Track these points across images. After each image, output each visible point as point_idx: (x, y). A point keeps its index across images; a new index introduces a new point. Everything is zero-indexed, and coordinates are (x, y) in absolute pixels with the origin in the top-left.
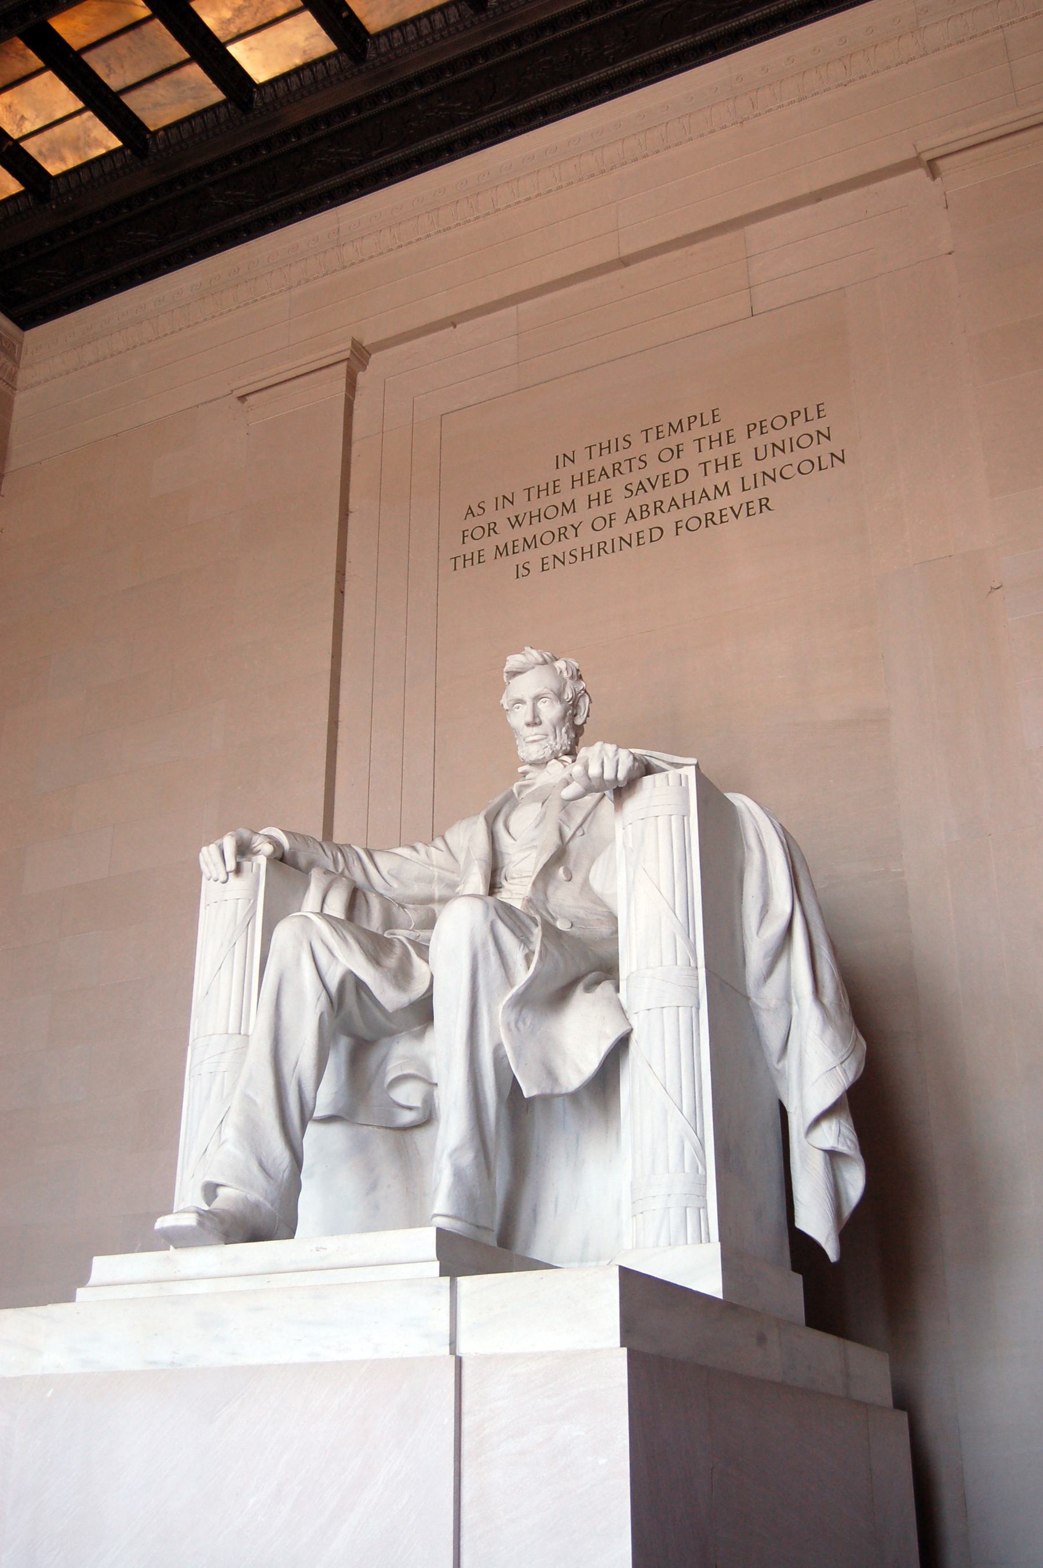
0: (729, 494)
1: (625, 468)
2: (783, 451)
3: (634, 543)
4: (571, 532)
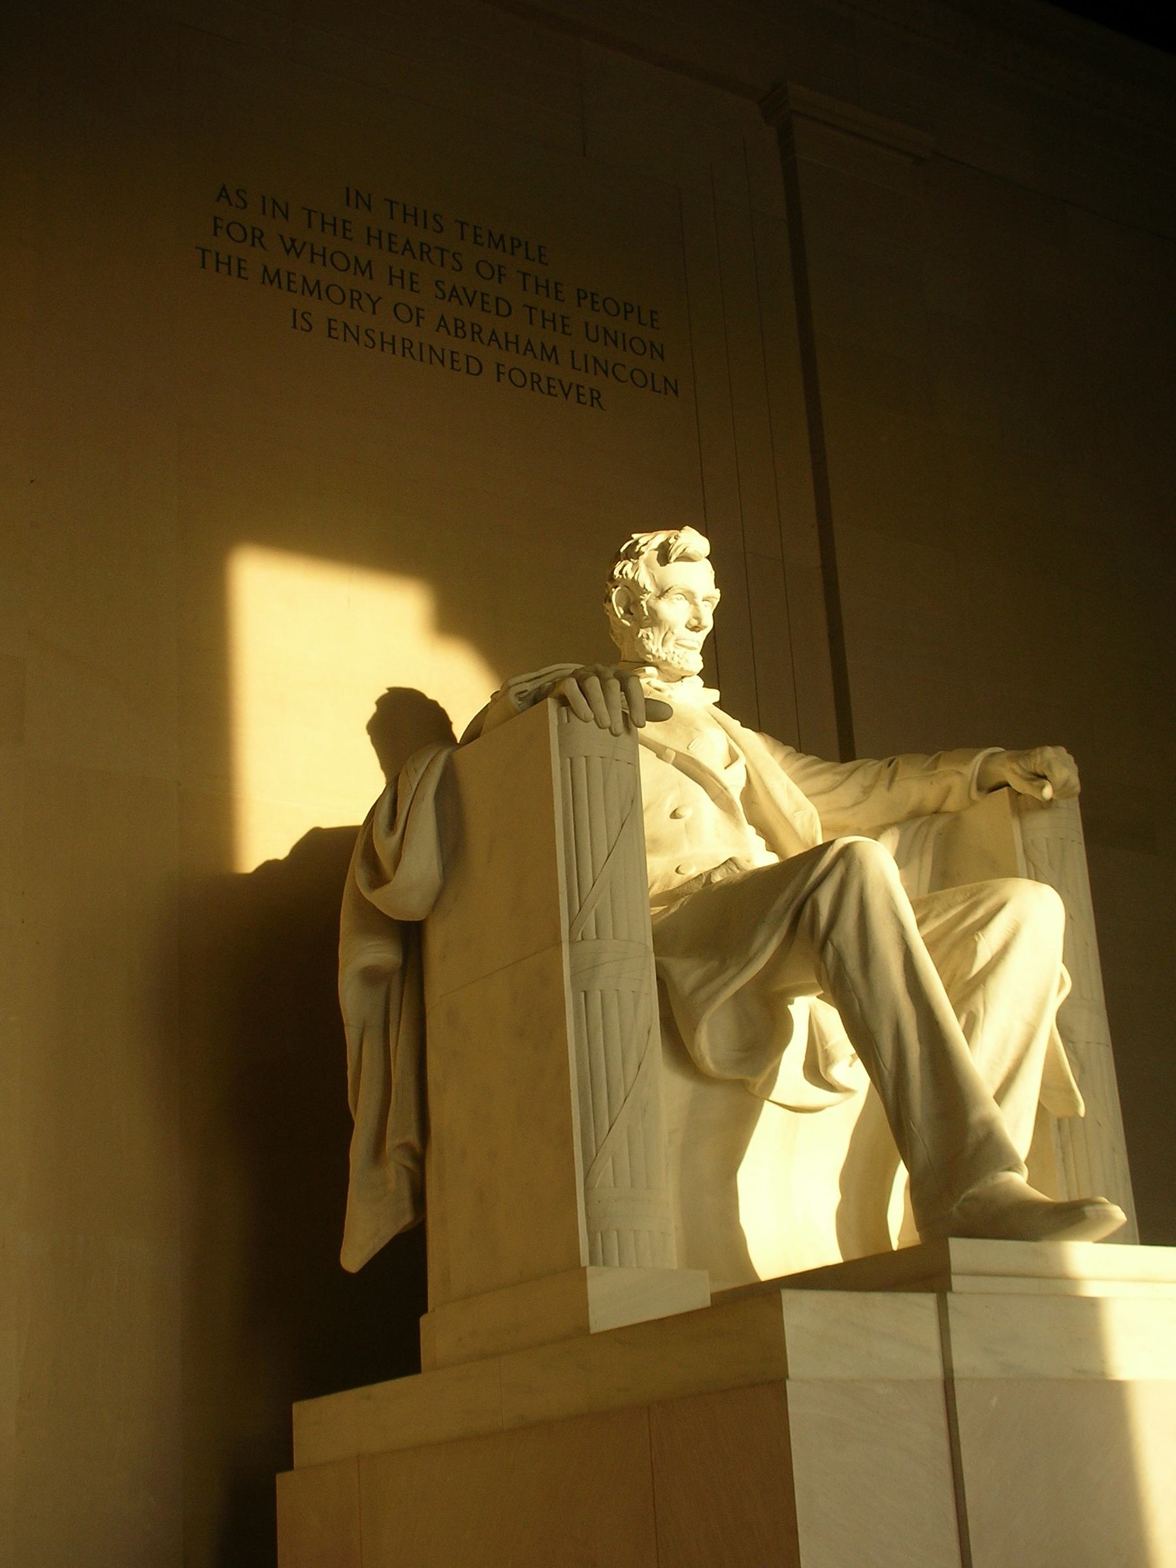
0: (557, 363)
1: (435, 255)
2: (615, 343)
3: (448, 362)
4: (366, 303)
